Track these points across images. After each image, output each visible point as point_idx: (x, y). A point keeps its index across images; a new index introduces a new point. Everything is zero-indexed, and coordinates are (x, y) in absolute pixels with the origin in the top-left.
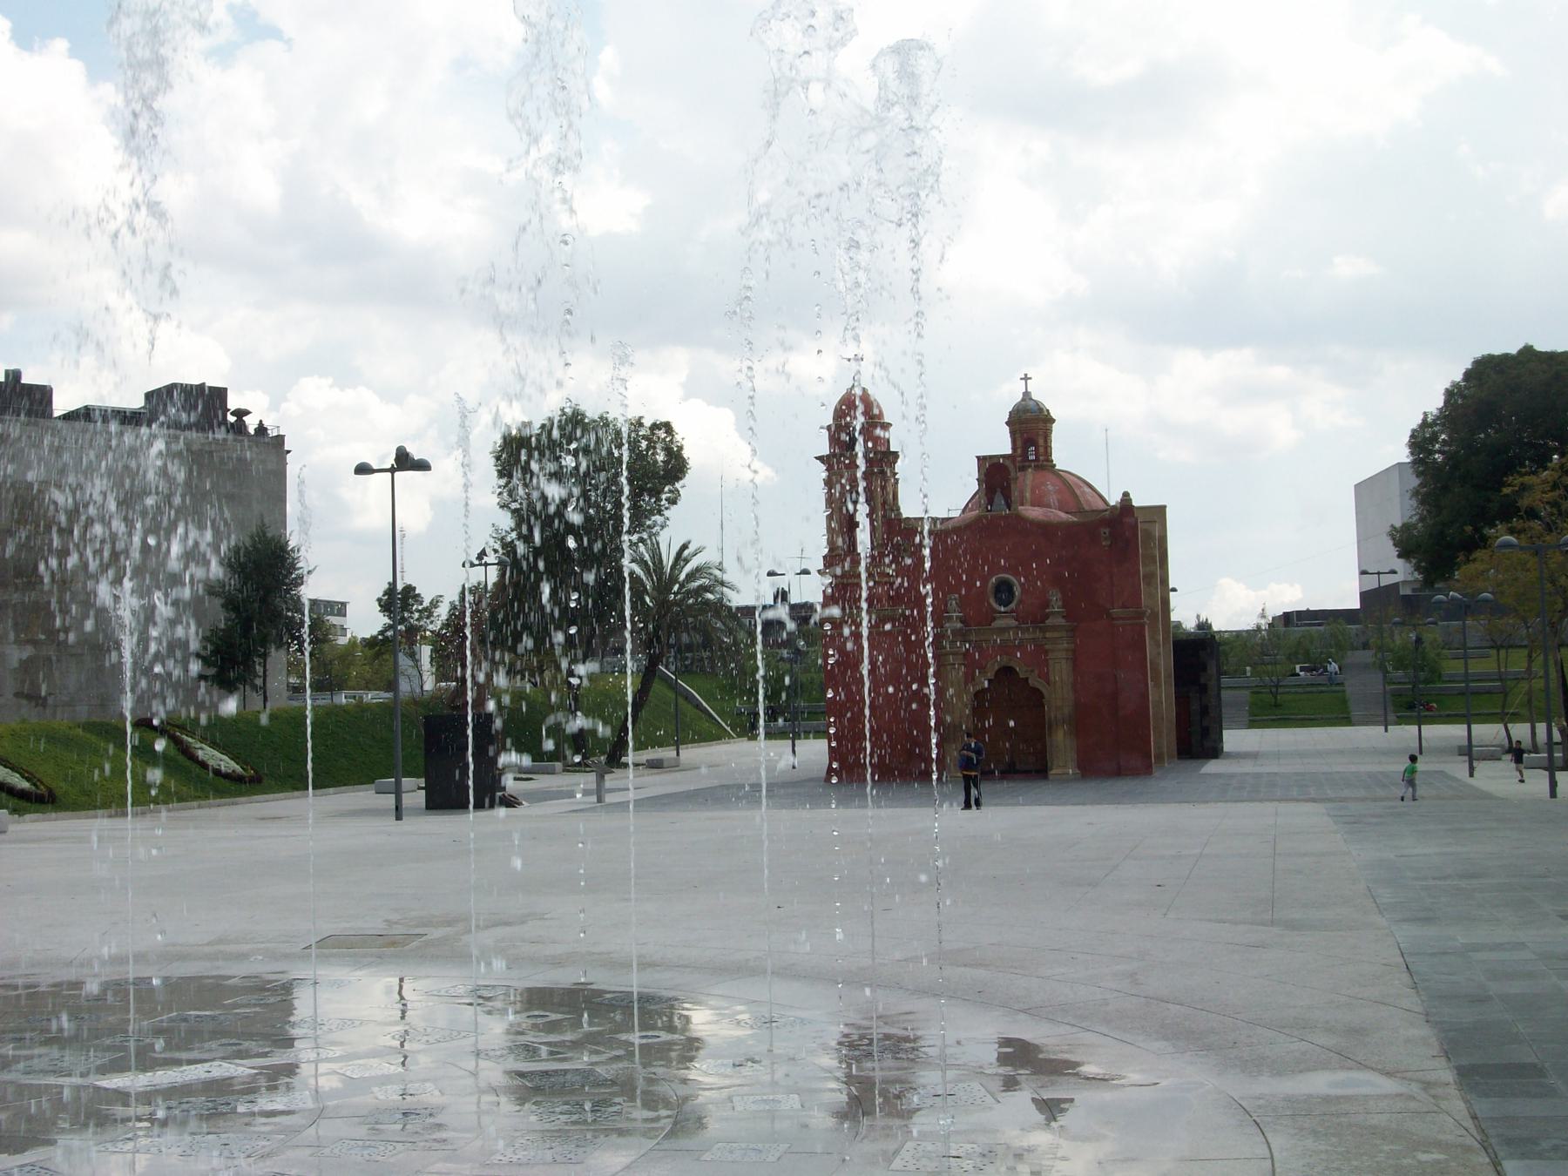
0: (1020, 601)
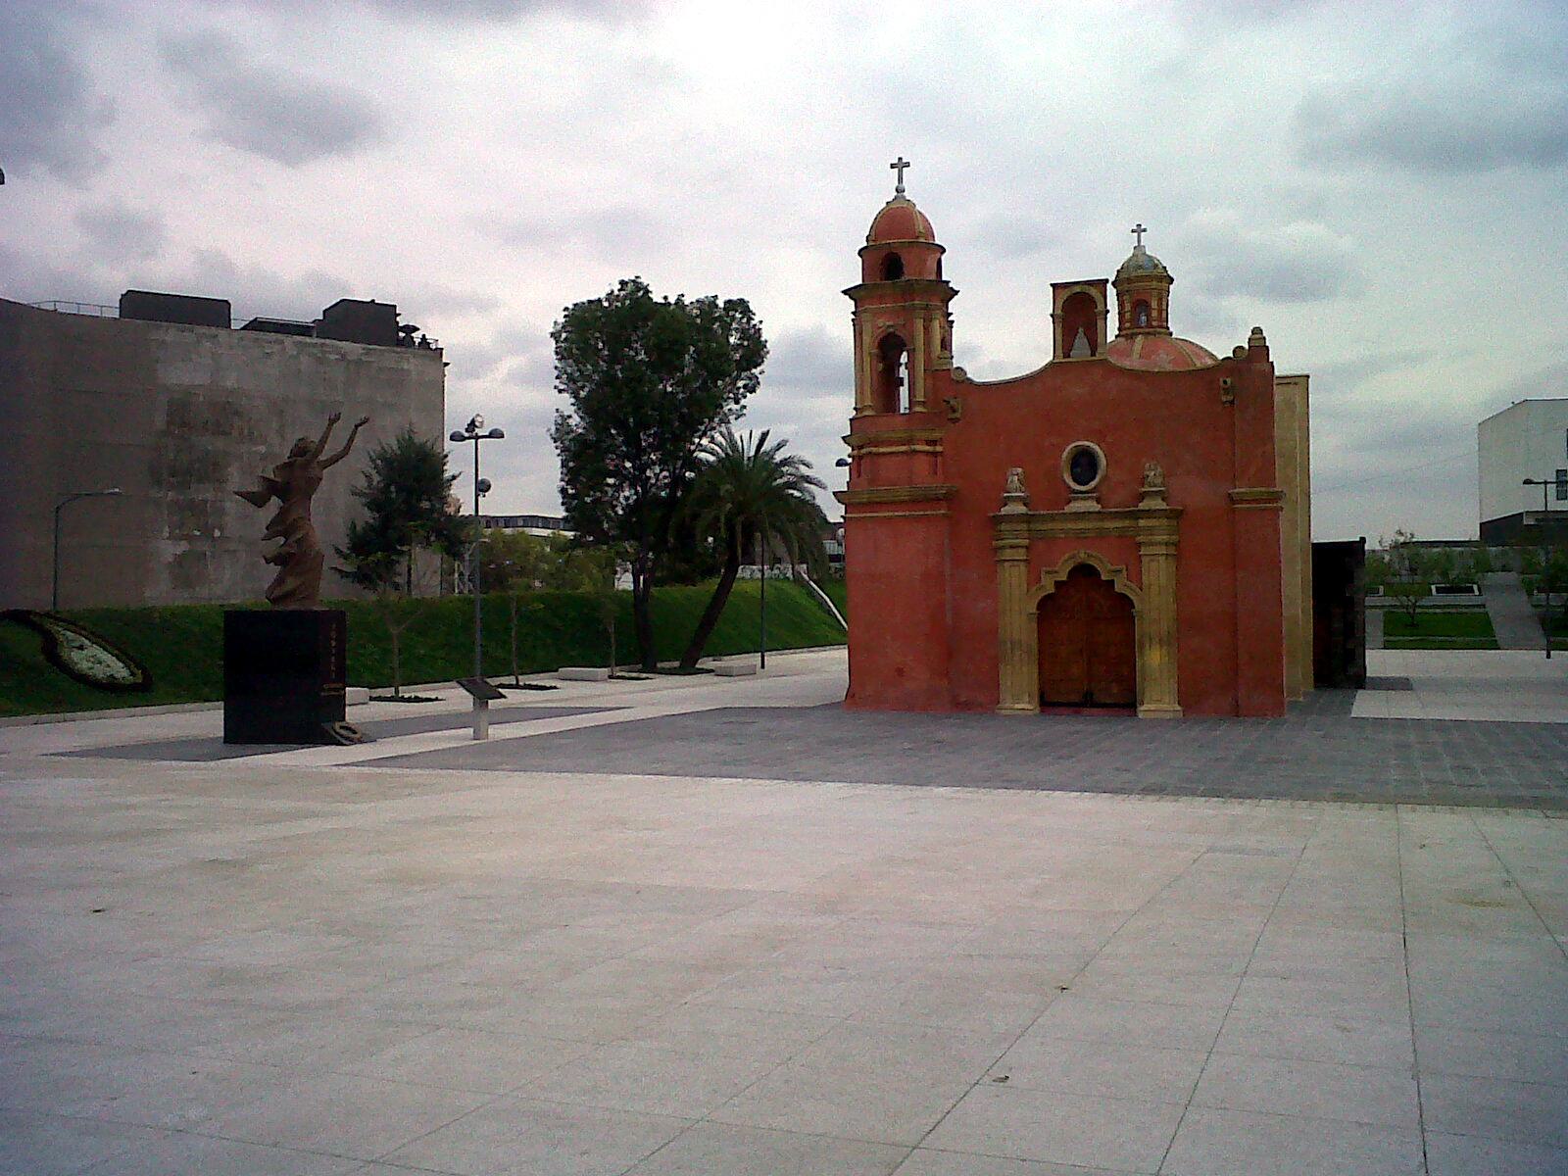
0: (1105, 478)
